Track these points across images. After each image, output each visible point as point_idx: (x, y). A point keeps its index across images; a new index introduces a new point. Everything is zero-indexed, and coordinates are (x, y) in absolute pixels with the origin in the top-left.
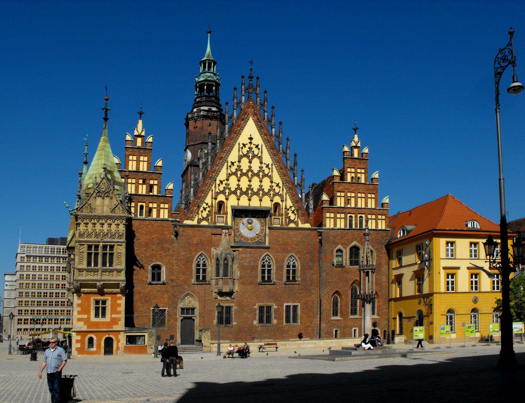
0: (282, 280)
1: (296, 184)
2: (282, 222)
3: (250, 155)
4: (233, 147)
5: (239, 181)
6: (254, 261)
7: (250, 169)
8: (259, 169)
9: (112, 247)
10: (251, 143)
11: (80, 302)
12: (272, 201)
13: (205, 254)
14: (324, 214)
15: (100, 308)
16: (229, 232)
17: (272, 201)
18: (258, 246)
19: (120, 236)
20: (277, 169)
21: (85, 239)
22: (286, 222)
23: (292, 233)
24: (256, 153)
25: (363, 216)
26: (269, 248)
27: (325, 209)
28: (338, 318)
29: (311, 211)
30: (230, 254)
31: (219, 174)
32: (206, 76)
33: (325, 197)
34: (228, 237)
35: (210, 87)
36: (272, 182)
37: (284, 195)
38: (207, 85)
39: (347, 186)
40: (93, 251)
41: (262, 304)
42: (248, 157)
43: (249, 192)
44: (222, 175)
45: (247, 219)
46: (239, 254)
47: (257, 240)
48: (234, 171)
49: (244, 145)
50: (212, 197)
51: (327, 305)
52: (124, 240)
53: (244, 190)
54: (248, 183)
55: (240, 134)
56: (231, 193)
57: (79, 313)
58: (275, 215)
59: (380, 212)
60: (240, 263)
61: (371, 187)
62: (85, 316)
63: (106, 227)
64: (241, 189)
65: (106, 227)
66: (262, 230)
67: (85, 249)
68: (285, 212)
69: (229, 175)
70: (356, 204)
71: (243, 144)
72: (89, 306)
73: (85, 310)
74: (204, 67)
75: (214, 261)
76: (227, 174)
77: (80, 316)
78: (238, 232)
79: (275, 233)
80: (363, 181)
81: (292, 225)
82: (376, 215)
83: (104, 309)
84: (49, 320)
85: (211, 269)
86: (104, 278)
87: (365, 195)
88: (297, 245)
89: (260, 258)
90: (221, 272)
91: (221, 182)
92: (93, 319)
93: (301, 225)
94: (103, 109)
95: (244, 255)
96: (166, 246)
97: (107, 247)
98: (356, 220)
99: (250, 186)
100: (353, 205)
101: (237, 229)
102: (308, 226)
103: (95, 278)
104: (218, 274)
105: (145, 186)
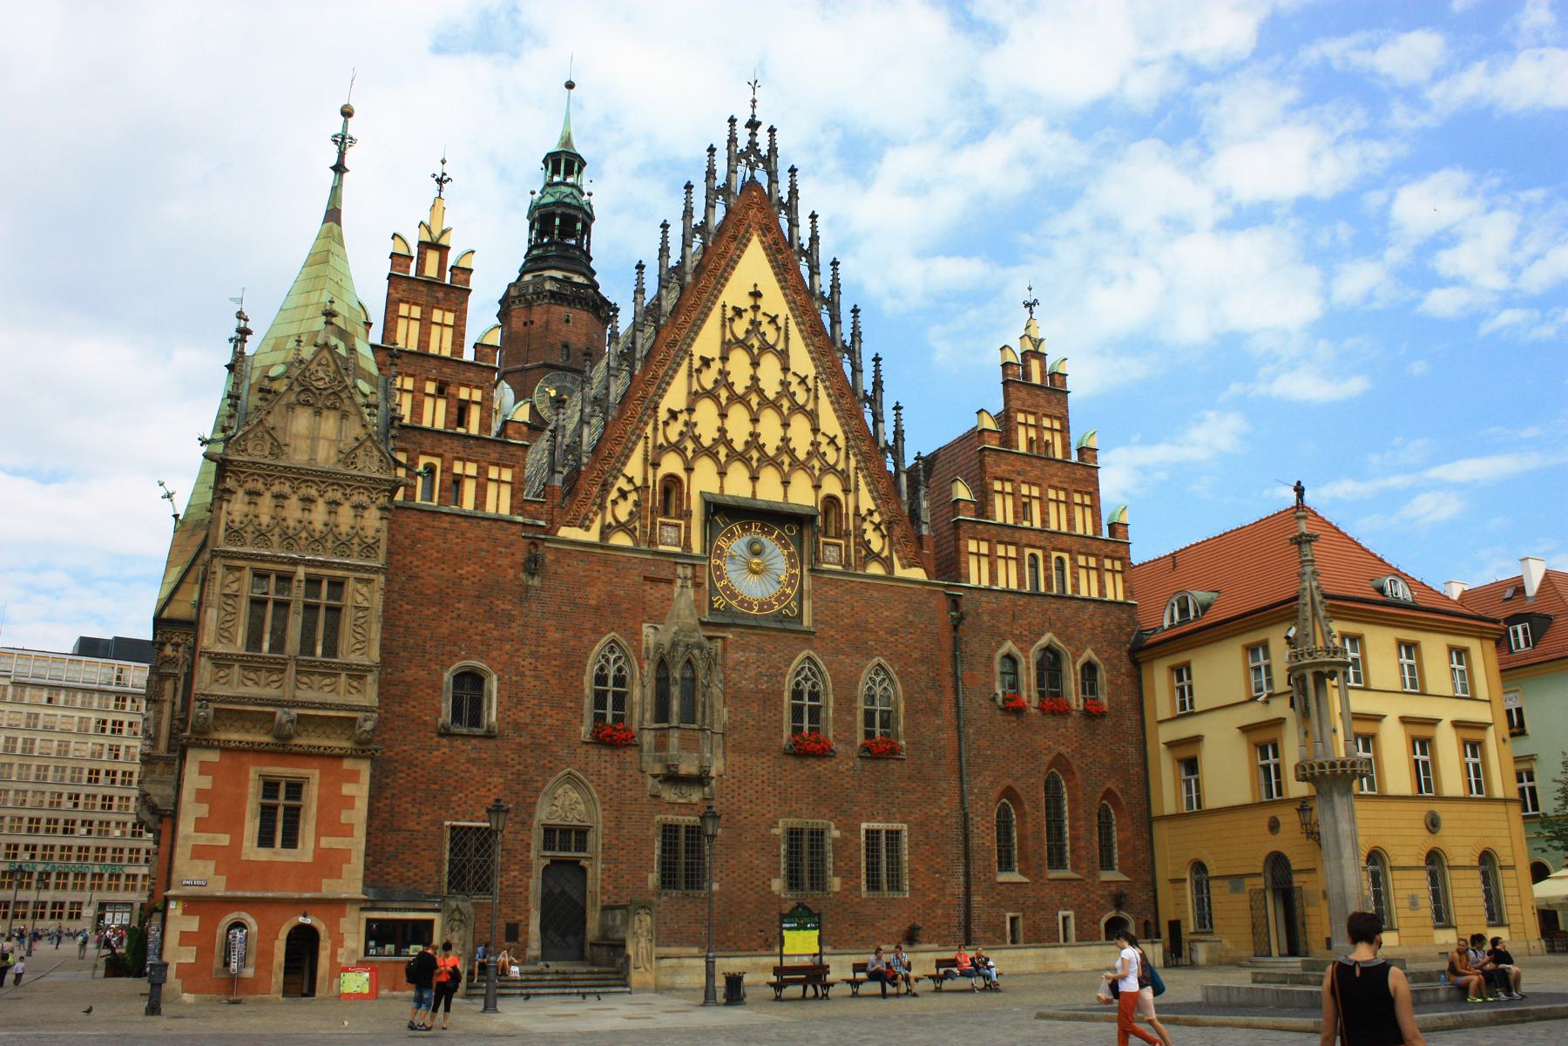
1: (882, 445)
2: (848, 556)
4: (707, 315)
5: (723, 416)
6: (771, 676)
7: (755, 385)
8: (779, 389)
9: (337, 585)
10: (756, 308)
11: (206, 782)
12: (817, 487)
13: (623, 642)
14: (962, 542)
15: (281, 811)
16: (694, 576)
17: (817, 487)
18: (779, 625)
20: (829, 395)
23: (876, 594)
24: (771, 336)
25: (1066, 556)
29: (925, 530)
30: (700, 647)
31: (665, 391)
33: (962, 492)
34: (691, 592)
36: (815, 430)
37: (852, 474)
42: (749, 349)
43: (753, 456)
44: (675, 396)
45: (747, 538)
46: (725, 649)
47: (777, 608)
48: (709, 385)
49: (739, 312)
50: (646, 460)
53: (739, 446)
54: (749, 428)
55: (727, 280)
56: (702, 451)
57: (201, 825)
58: (826, 535)
59: (1108, 550)
60: (726, 681)
62: (224, 840)
63: (319, 514)
64: (729, 444)
65: (319, 514)
66: (793, 576)
67: (245, 585)
70: (1044, 521)
71: (734, 308)
72: (241, 800)
73: (224, 816)
75: (649, 668)
76: (690, 393)
77: (204, 839)
78: (720, 578)
80: (1059, 455)
81: (875, 569)
83: (293, 816)
85: (640, 694)
86: (304, 694)
87: (1067, 495)
88: (893, 632)
89: (788, 666)
90: (675, 705)
91: (673, 415)
92: (252, 851)
93: (899, 572)
95: (739, 656)
96: (501, 605)
97: (320, 582)
99: (755, 435)
100: (1037, 524)
101: (718, 568)
102: (918, 574)
103: (270, 692)
104: (662, 713)
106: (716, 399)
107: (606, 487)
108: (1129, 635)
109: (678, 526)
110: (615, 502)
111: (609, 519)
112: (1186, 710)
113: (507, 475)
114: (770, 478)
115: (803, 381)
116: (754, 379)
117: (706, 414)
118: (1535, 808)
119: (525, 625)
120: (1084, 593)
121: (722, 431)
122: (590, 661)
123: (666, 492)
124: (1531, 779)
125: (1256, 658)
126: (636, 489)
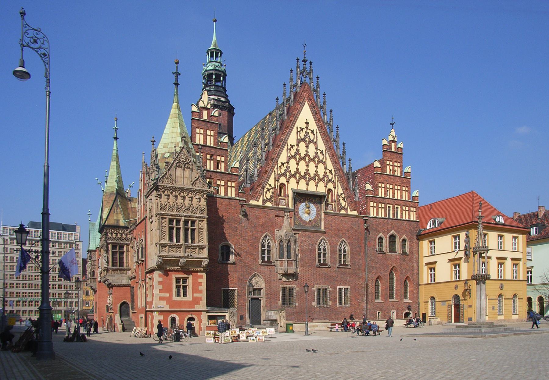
0: (335, 264)
2: (335, 208)
3: (307, 139)
7: (307, 155)
9: (193, 223)
12: (326, 186)
13: (270, 235)
17: (326, 186)
19: (202, 212)
21: (167, 212)
22: (338, 209)
25: (399, 207)
26: (324, 232)
27: (370, 198)
28: (379, 301)
32: (215, 65)
33: (368, 187)
35: (218, 76)
36: (325, 168)
38: (216, 75)
39: (387, 178)
40: (174, 225)
41: (319, 286)
42: (305, 141)
43: (306, 177)
44: (283, 158)
48: (293, 154)
51: (371, 289)
52: (205, 215)
53: (303, 174)
54: (306, 167)
61: (405, 181)
66: (318, 214)
68: (337, 199)
69: (289, 158)
74: (212, 56)
79: (330, 218)
81: (343, 212)
82: (409, 207)
84: (35, 302)
88: (347, 231)
91: (283, 164)
93: (350, 213)
94: (174, 73)
98: (393, 211)
102: (355, 213)
104: (281, 256)
105: (212, 162)
106: (295, 158)
107: (263, 188)
108: (416, 231)
109: (285, 199)
110: (266, 192)
111: (265, 198)
112: (433, 253)
113: (233, 184)
114: (312, 183)
115: (322, 152)
116: (307, 151)
117: (293, 162)
118: (531, 282)
119: (241, 231)
120: (404, 218)
121: (297, 169)
122: (261, 241)
123: (281, 189)
124: (531, 273)
125: (455, 239)
126: (272, 188)
